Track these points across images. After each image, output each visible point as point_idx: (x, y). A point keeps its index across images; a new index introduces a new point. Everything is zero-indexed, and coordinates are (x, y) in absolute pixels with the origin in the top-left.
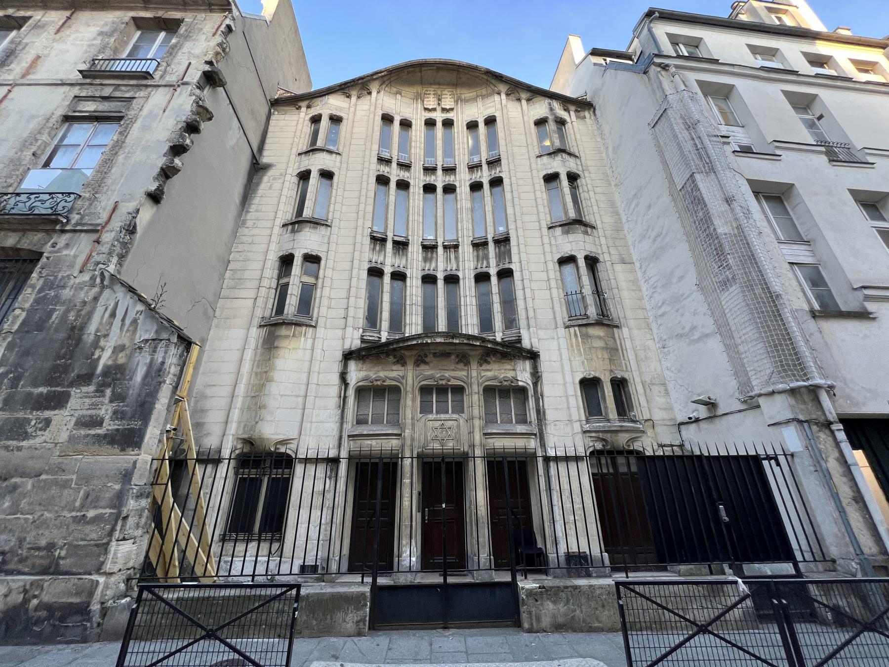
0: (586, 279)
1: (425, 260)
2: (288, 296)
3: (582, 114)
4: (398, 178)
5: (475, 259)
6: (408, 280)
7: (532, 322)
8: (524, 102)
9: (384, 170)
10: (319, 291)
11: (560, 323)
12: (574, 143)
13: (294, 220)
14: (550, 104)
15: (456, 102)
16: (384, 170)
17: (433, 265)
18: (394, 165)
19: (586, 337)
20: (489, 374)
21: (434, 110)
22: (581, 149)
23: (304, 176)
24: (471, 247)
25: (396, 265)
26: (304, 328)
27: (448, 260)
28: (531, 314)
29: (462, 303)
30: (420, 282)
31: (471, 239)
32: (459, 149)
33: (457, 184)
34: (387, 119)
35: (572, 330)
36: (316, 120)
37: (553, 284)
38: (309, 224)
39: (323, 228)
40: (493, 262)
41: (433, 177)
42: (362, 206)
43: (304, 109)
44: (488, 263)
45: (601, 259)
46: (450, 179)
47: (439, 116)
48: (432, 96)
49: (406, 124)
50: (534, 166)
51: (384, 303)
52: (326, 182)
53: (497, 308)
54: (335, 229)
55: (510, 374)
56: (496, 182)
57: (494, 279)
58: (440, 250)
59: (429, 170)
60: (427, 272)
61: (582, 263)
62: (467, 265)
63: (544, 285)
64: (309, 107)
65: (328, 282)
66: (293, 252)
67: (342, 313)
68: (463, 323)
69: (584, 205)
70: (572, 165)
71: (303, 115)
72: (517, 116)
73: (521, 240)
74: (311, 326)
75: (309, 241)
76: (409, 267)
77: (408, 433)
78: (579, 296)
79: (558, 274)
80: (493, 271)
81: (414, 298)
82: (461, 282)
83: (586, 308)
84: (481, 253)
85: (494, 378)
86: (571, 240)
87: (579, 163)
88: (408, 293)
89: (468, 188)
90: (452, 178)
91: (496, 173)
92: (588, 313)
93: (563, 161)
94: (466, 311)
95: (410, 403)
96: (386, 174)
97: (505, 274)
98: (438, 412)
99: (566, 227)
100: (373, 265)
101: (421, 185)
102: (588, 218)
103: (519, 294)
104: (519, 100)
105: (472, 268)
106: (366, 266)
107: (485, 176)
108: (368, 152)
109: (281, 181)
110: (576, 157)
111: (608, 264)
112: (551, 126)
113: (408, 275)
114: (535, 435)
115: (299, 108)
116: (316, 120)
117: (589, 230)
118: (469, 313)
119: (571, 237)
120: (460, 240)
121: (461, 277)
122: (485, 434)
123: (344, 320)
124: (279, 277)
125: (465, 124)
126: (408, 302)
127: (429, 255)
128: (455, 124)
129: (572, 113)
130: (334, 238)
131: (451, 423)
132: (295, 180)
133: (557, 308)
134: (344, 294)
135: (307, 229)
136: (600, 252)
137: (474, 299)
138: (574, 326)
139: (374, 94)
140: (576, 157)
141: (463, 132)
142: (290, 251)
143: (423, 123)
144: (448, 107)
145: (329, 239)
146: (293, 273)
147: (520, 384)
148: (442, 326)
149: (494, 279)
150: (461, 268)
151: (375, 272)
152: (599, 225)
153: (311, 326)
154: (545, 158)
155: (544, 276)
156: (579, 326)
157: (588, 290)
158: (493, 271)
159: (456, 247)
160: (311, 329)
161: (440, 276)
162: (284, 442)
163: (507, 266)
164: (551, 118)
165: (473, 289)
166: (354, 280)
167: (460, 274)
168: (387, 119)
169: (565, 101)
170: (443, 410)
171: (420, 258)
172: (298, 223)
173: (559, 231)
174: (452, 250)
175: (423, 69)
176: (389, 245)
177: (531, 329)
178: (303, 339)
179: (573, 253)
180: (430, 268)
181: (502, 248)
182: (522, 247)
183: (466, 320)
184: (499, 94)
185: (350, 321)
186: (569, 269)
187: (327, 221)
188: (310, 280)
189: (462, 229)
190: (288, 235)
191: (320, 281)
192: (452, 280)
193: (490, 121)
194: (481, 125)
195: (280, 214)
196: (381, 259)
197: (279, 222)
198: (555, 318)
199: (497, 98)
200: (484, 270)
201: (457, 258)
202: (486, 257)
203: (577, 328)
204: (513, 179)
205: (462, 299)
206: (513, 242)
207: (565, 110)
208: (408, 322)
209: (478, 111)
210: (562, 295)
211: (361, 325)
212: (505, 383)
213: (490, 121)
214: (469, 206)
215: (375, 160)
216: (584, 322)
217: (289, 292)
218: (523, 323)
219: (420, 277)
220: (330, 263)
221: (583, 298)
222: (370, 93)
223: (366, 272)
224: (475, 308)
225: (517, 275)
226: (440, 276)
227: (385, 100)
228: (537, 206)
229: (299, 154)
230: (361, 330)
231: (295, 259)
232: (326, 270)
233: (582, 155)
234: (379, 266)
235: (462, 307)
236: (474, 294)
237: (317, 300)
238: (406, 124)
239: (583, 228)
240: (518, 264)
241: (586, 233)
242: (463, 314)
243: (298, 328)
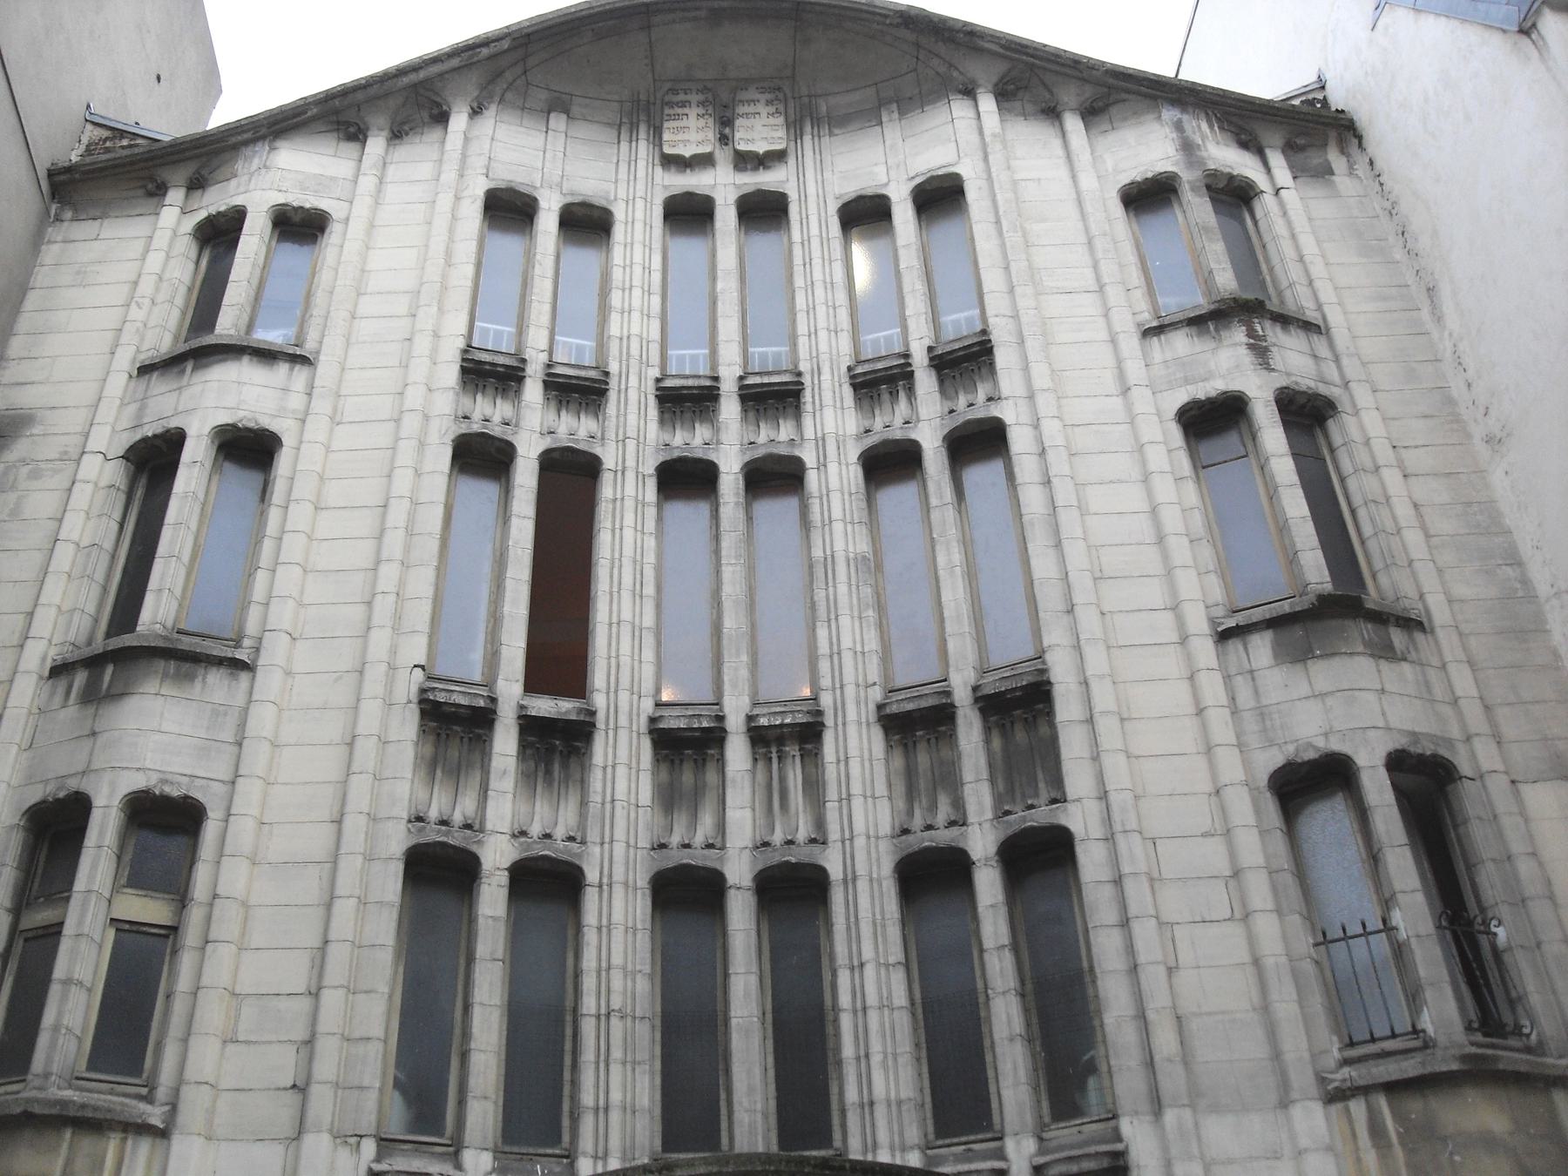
0: (1402, 866)
1: (669, 799)
2: (55, 990)
3: (1314, 159)
4: (546, 443)
5: (900, 788)
6: (591, 899)
7: (1172, 1080)
8: (1073, 123)
9: (489, 412)
10: (187, 961)
11: (1302, 1079)
12: (1295, 273)
13: (99, 646)
14: (1179, 127)
15: (795, 128)
16: (489, 412)
17: (705, 828)
18: (533, 391)
19: (1421, 1136)
21: (704, 161)
22: (1327, 294)
23: (154, 461)
24: (877, 734)
25: (536, 830)
26: (112, 1144)
27: (773, 799)
28: (1165, 1041)
29: (845, 1000)
30: (642, 905)
31: (876, 694)
32: (811, 310)
33: (809, 457)
34: (508, 209)
35: (1358, 1107)
36: (219, 235)
37: (1259, 892)
38: (160, 664)
40: (979, 796)
41: (702, 433)
42: (389, 575)
43: (175, 196)
44: (958, 804)
45: (1465, 768)
46: (776, 436)
47: (724, 186)
48: (693, 112)
49: (587, 224)
50: (1135, 370)
51: (477, 1013)
52: (241, 480)
53: (1006, 1017)
54: (269, 681)
56: (979, 442)
57: (988, 884)
58: (737, 752)
59: (685, 401)
60: (675, 858)
61: (1377, 788)
62: (861, 815)
63: (1218, 901)
64: (196, 185)
65: (227, 923)
66: (86, 786)
67: (285, 1067)
68: (852, 1095)
69: (1367, 530)
70: (1295, 361)
71: (173, 221)
72: (1046, 196)
73: (1103, 697)
74: (143, 1129)
75: (157, 737)
76: (593, 835)
78: (1380, 943)
79: (1279, 842)
80: (981, 842)
81: (617, 982)
82: (837, 897)
83: (1414, 997)
84: (923, 759)
86: (1322, 684)
87: (1324, 351)
88: (589, 960)
89: (855, 473)
90: (786, 431)
91: (972, 405)
92: (1426, 1022)
93: (1260, 352)
94: (861, 1037)
96: (496, 430)
97: (1041, 857)
99: (1298, 632)
100: (433, 835)
101: (650, 468)
102: (1387, 584)
103: (1106, 948)
104: (1052, 113)
105: (886, 827)
106: (397, 841)
107: (926, 419)
108: (422, 344)
109: (61, 481)
110: (1308, 327)
111: (1498, 786)
112: (1197, 208)
113: (592, 875)
115: (158, 191)
116: (219, 235)
117: (1397, 637)
118: (876, 1047)
119: (1324, 673)
120: (826, 700)
121: (835, 870)
123: (292, 1098)
124: (22, 901)
125: (833, 207)
126: (589, 1004)
127: (687, 777)
128: (793, 210)
129: (1277, 160)
130: (262, 720)
132: (115, 473)
133: (1286, 1006)
134: (296, 975)
135: (151, 685)
136: (1455, 732)
137: (898, 980)
138: (1365, 1090)
139: (459, 120)
140: (1308, 327)
141: (825, 241)
142: (73, 784)
143: (658, 212)
144: (761, 148)
145: (242, 725)
146: (80, 885)
148: (751, 1117)
149: (988, 884)
150: (834, 832)
151: (439, 871)
152: (1440, 614)
153: (143, 1129)
154: (1181, 343)
155: (1214, 856)
156: (1392, 1088)
157: (1414, 914)
158: (981, 842)
159: (808, 734)
160: (143, 1148)
161: (739, 871)
163: (1042, 816)
164: (1188, 177)
165: (894, 932)
166: (345, 910)
167: (833, 864)
168: (508, 209)
169: (1240, 116)
171: (646, 793)
172: (113, 662)
173: (1261, 646)
174: (793, 750)
175: (657, 19)
176: (505, 742)
177: (1170, 1116)
179: (1336, 746)
180: (690, 838)
181: (1020, 735)
182: (1107, 728)
183: (865, 1080)
184: (969, 92)
185: (322, 1102)
186: (1327, 820)
187: (238, 644)
188: (148, 909)
189: (836, 654)
190: (72, 711)
191: (195, 915)
192: (794, 891)
193: (940, 197)
194: (903, 214)
195: (44, 623)
196: (466, 807)
197: (37, 656)
198: (1277, 1056)
199: (960, 108)
200: (943, 837)
201: (814, 788)
202: (948, 779)
203: (1382, 1102)
204: (1051, 428)
205: (844, 979)
206: (1066, 708)
207: (1244, 145)
208: (587, 1099)
209: (890, 159)
210: (1304, 943)
211: (368, 1122)
213: (940, 197)
214: (863, 546)
215: (450, 374)
216: (1409, 1068)
217: (59, 972)
218: (1127, 1080)
219: (643, 881)
220: (243, 832)
221: (1400, 952)
222: (442, 118)
223: (399, 867)
224: (903, 1020)
225: (1091, 861)
226: (739, 871)
227: (501, 145)
228: (1161, 540)
229: (145, 370)
230: (369, 1148)
231: (96, 817)
232: (227, 870)
233: (1335, 318)
234: (456, 839)
235: (846, 1022)
236: (896, 953)
237: (179, 1007)
238: (587, 224)
239: (1367, 629)
240: (1093, 807)
241: (1385, 652)
242: (848, 1051)
243: (87, 1143)
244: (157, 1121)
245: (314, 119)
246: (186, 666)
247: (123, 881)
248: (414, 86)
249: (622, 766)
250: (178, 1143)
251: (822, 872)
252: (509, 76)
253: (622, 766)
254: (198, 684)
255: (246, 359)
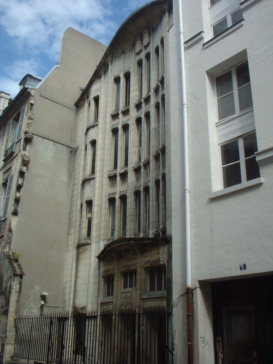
4: (122, 125)
20: (146, 259)
39: (92, 181)
43: (86, 101)
55: (155, 257)
77: (115, 300)
85: (149, 262)
95: (118, 283)
98: (130, 287)
114: (165, 297)
122: (143, 299)
131: (129, 294)
147: (161, 263)
162: (84, 308)
170: (131, 286)
178: (87, 252)
188: (89, 216)
212: (154, 264)
244: (90, 243)
245: (95, 78)
246: (89, 181)
247: (88, 212)
248: (103, 64)
249: (131, 176)
250: (91, 244)
251: (149, 186)
252: (115, 52)
253: (131, 176)
254: (90, 183)
255: (92, 128)
